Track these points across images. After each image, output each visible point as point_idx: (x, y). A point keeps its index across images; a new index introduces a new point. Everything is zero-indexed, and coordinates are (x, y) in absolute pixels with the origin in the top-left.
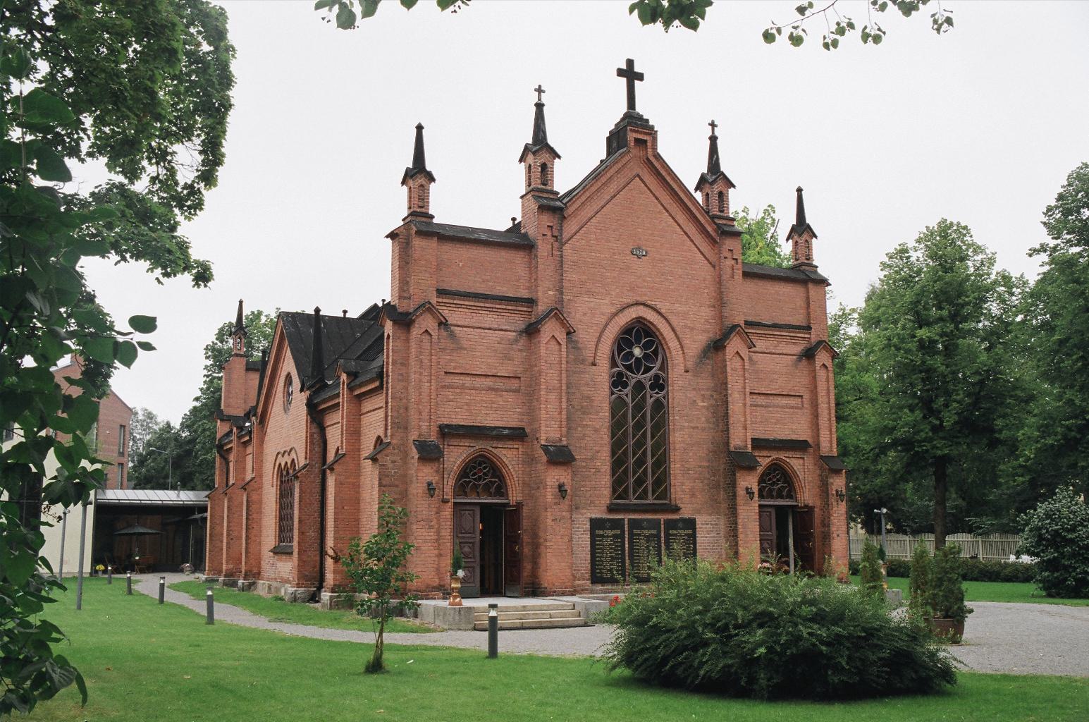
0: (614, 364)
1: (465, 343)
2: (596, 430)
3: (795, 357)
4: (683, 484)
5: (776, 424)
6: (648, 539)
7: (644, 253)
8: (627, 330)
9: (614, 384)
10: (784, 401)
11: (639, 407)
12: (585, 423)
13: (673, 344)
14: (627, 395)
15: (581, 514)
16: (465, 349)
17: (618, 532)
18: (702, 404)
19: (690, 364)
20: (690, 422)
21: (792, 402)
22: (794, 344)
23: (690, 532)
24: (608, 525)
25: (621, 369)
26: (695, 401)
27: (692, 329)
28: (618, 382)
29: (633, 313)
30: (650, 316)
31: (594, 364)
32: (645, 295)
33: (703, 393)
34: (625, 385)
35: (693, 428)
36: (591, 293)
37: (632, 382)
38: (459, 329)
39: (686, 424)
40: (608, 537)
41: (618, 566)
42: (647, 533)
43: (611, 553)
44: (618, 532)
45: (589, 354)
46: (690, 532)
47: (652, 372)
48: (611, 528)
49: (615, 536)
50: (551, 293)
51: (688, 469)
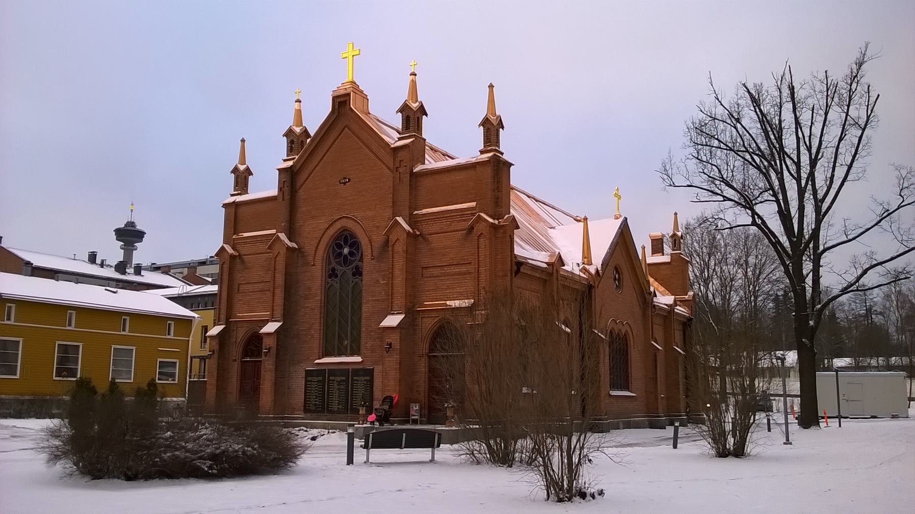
0: (330, 263)
2: (313, 309)
3: (465, 232)
4: (366, 343)
5: (446, 289)
6: (339, 383)
7: (347, 180)
9: (330, 276)
10: (456, 270)
12: (306, 305)
13: (364, 242)
14: (337, 283)
15: (301, 366)
16: (248, 268)
17: (321, 378)
18: (382, 282)
21: (463, 269)
22: (464, 220)
23: (368, 378)
25: (334, 265)
27: (378, 227)
28: (333, 274)
29: (338, 225)
30: (350, 224)
31: (314, 265)
33: (383, 273)
35: (375, 300)
38: (246, 257)
39: (370, 299)
41: (320, 402)
42: (339, 379)
43: (316, 393)
44: (321, 378)
45: (311, 258)
46: (368, 378)
47: (354, 265)
49: (318, 381)
50: (283, 224)
51: (371, 331)
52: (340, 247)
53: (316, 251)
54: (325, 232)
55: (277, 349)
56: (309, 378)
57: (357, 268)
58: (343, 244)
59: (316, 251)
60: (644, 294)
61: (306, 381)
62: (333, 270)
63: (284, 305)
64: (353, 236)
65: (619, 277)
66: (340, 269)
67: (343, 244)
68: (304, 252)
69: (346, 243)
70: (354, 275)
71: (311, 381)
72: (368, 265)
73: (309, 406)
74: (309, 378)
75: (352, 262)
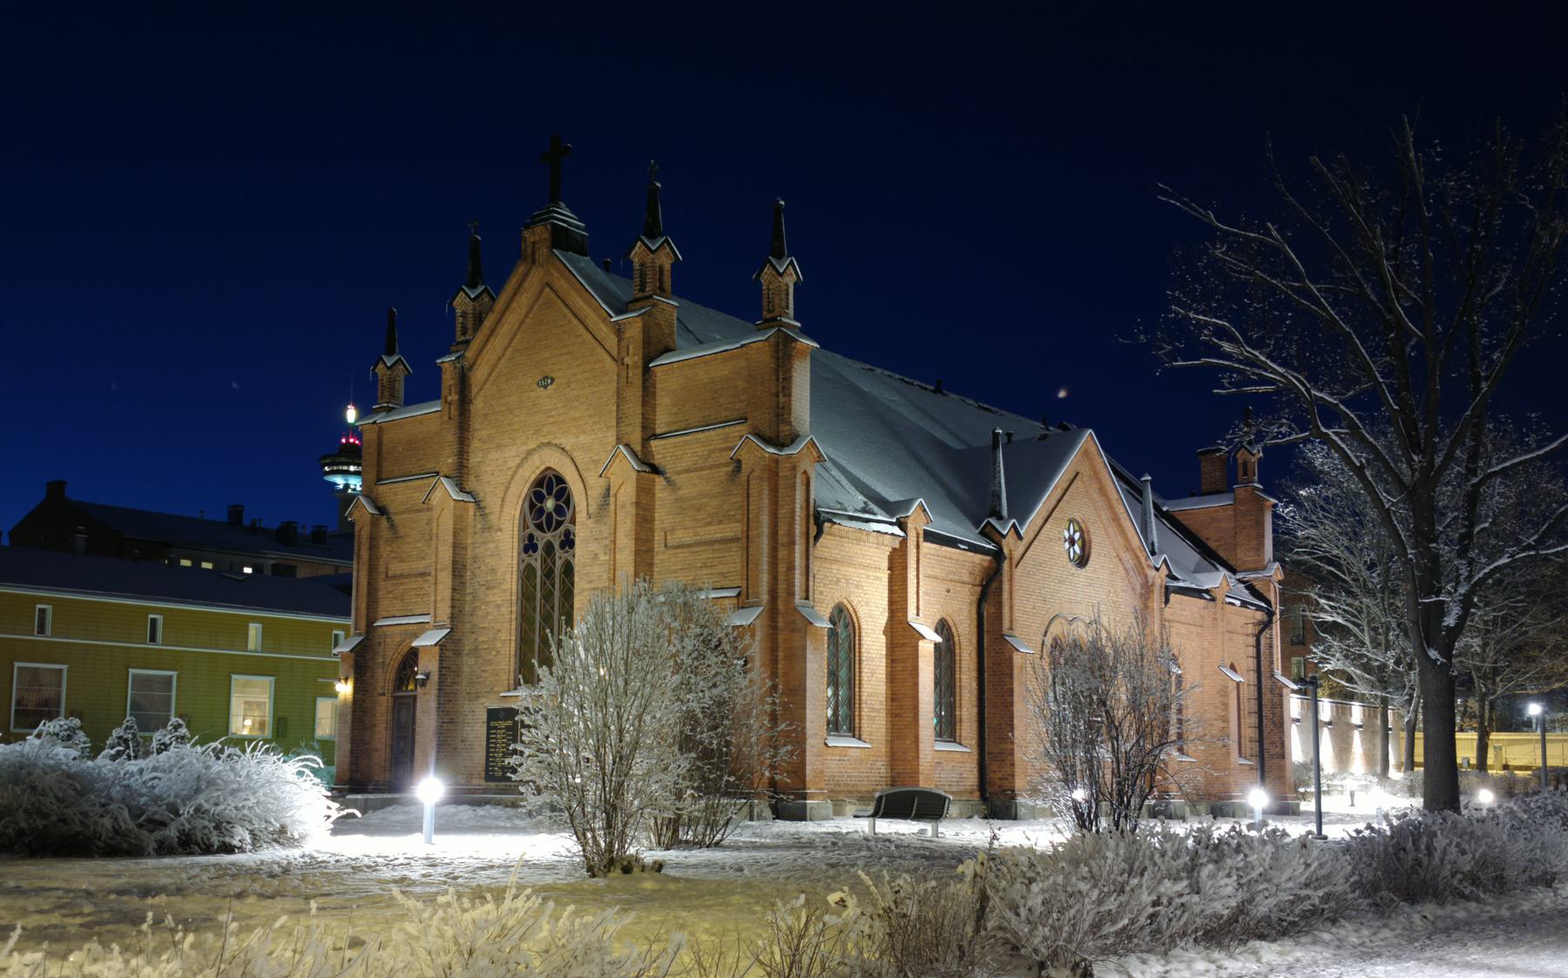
0: (525, 527)
1: (402, 531)
2: (498, 606)
8: (539, 483)
11: (549, 574)
19: (593, 509)
20: (591, 582)
24: (502, 715)
25: (532, 529)
26: (596, 555)
28: (529, 546)
32: (549, 433)
34: (535, 549)
35: (594, 589)
36: (499, 447)
37: (541, 545)
40: (501, 729)
45: (493, 518)
47: (562, 529)
48: (505, 720)
49: (507, 728)
50: (450, 460)
52: (540, 497)
53: (502, 506)
54: (515, 472)
55: (441, 675)
56: (492, 724)
57: (568, 533)
58: (544, 491)
59: (502, 506)
60: (1143, 568)
61: (489, 728)
62: (531, 537)
63: (453, 600)
64: (560, 480)
65: (1082, 537)
66: (542, 538)
67: (544, 491)
68: (485, 508)
69: (550, 493)
70: (562, 546)
71: (496, 728)
72: (583, 530)
73: (493, 771)
74: (492, 724)
75: (559, 524)
